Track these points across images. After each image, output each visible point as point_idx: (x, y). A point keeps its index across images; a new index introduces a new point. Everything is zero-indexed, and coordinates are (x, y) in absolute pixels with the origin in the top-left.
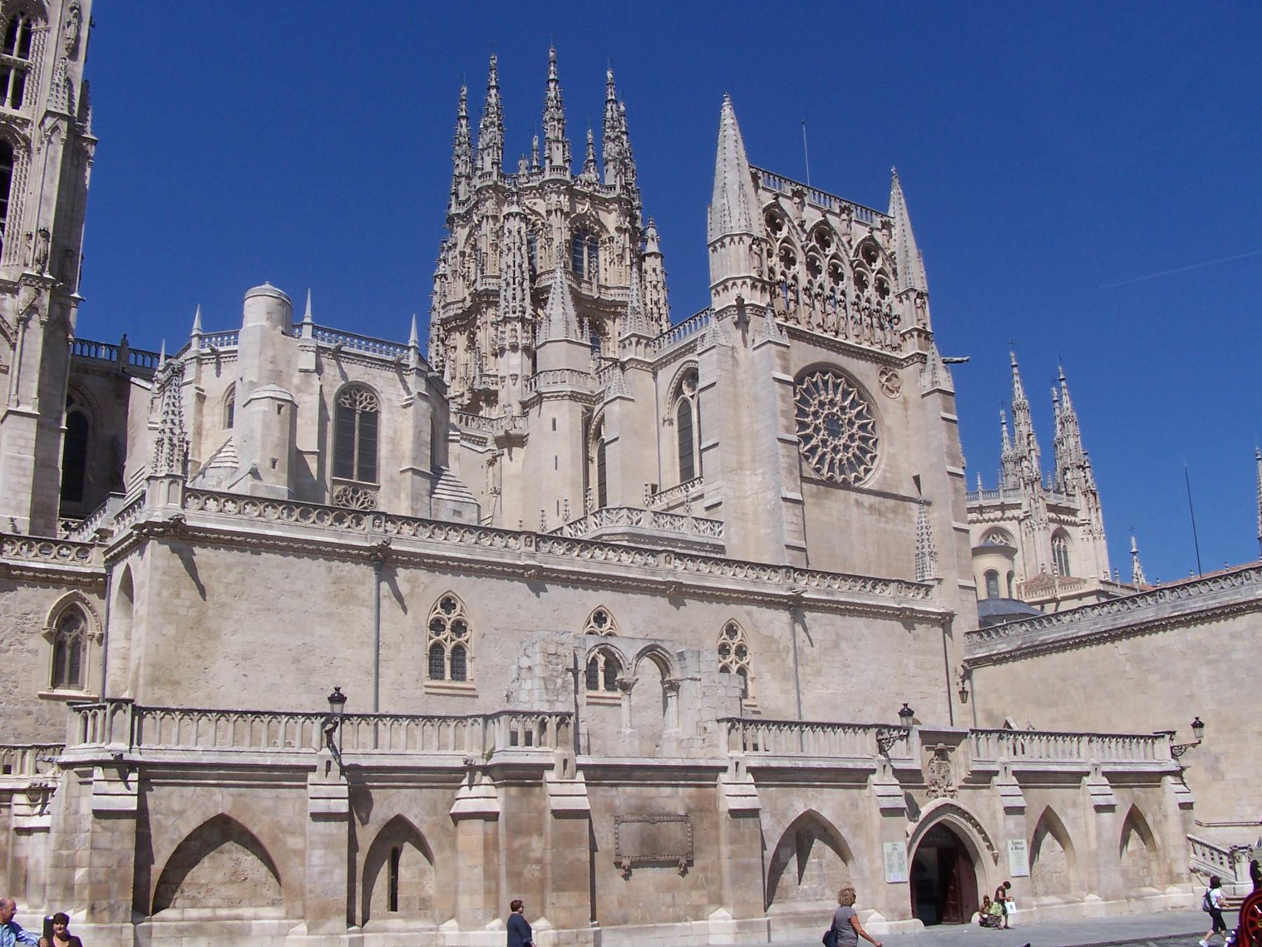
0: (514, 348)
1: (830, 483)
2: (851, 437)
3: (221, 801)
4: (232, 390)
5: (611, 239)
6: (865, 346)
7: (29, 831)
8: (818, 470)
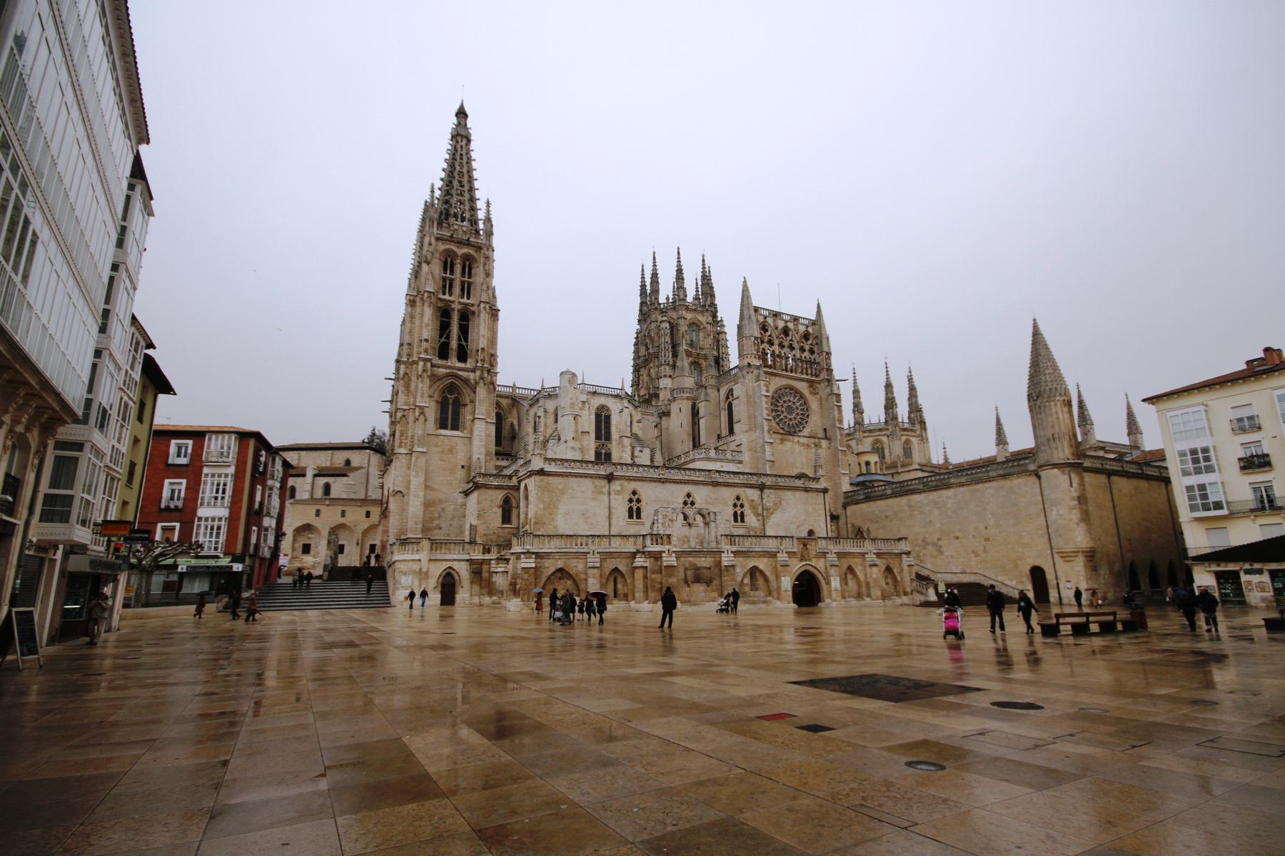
0: (665, 376)
1: (789, 433)
2: (797, 414)
3: (560, 564)
4: (556, 409)
5: (705, 328)
6: (804, 376)
7: (496, 572)
8: (783, 429)
